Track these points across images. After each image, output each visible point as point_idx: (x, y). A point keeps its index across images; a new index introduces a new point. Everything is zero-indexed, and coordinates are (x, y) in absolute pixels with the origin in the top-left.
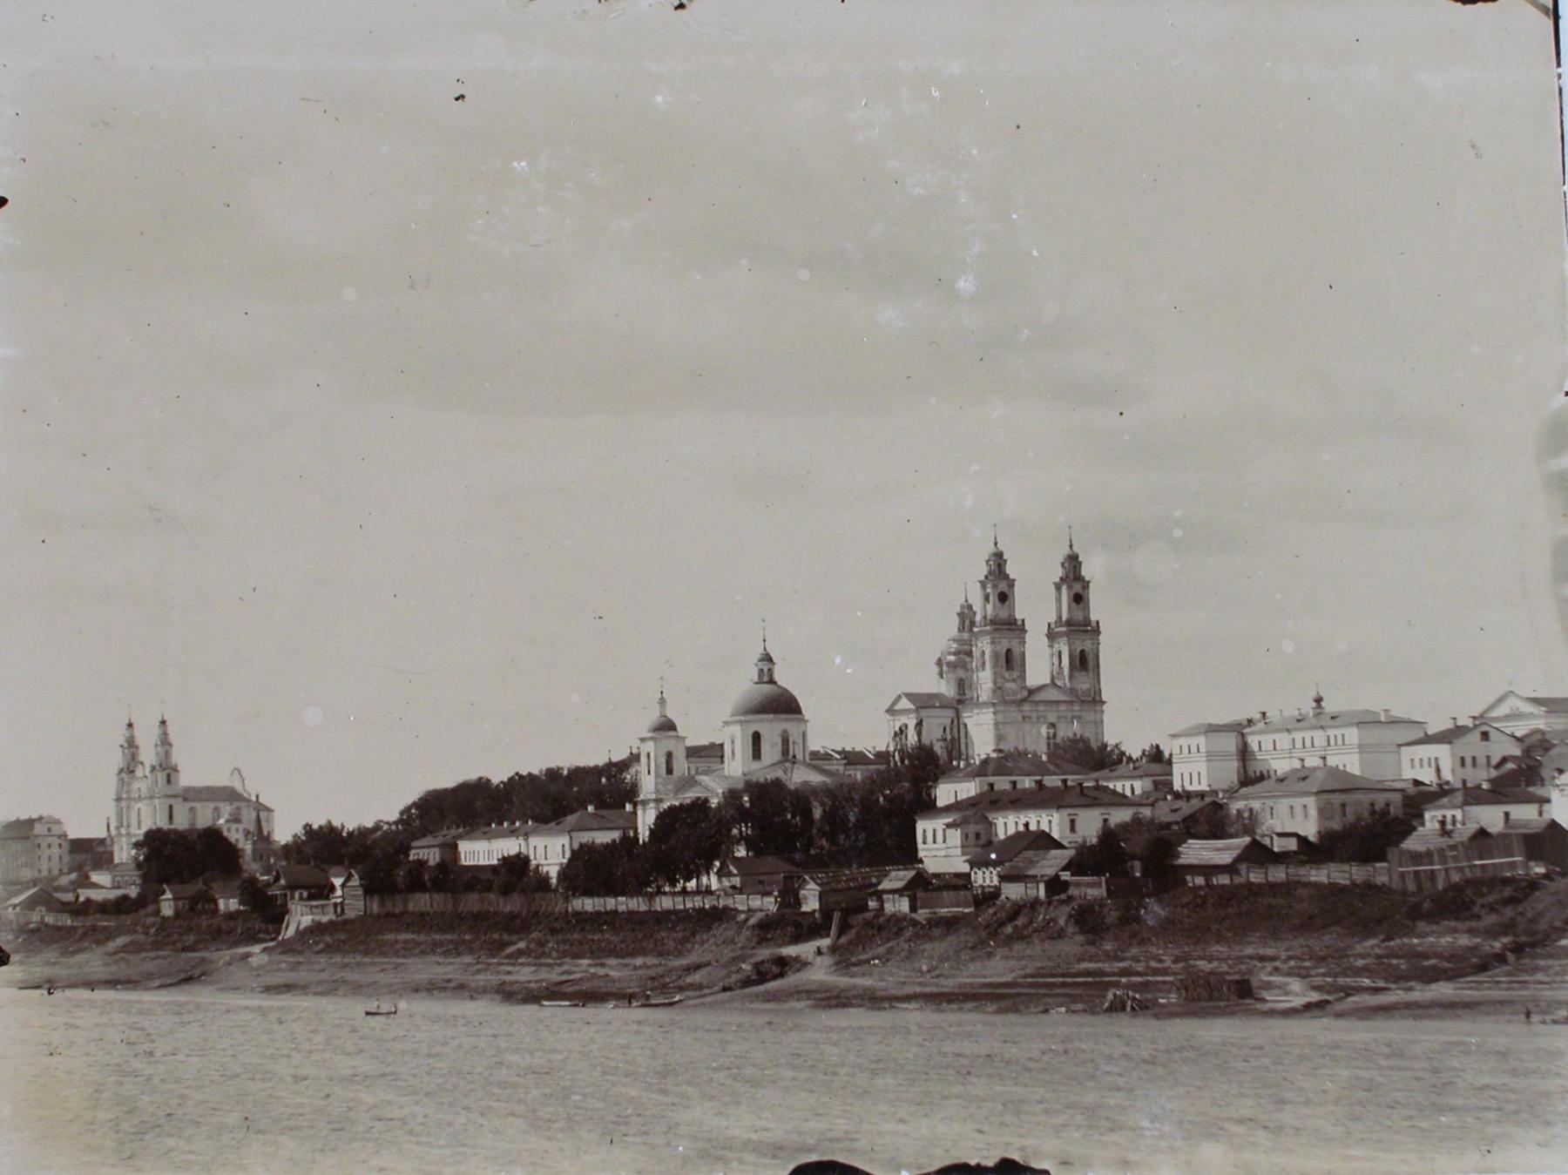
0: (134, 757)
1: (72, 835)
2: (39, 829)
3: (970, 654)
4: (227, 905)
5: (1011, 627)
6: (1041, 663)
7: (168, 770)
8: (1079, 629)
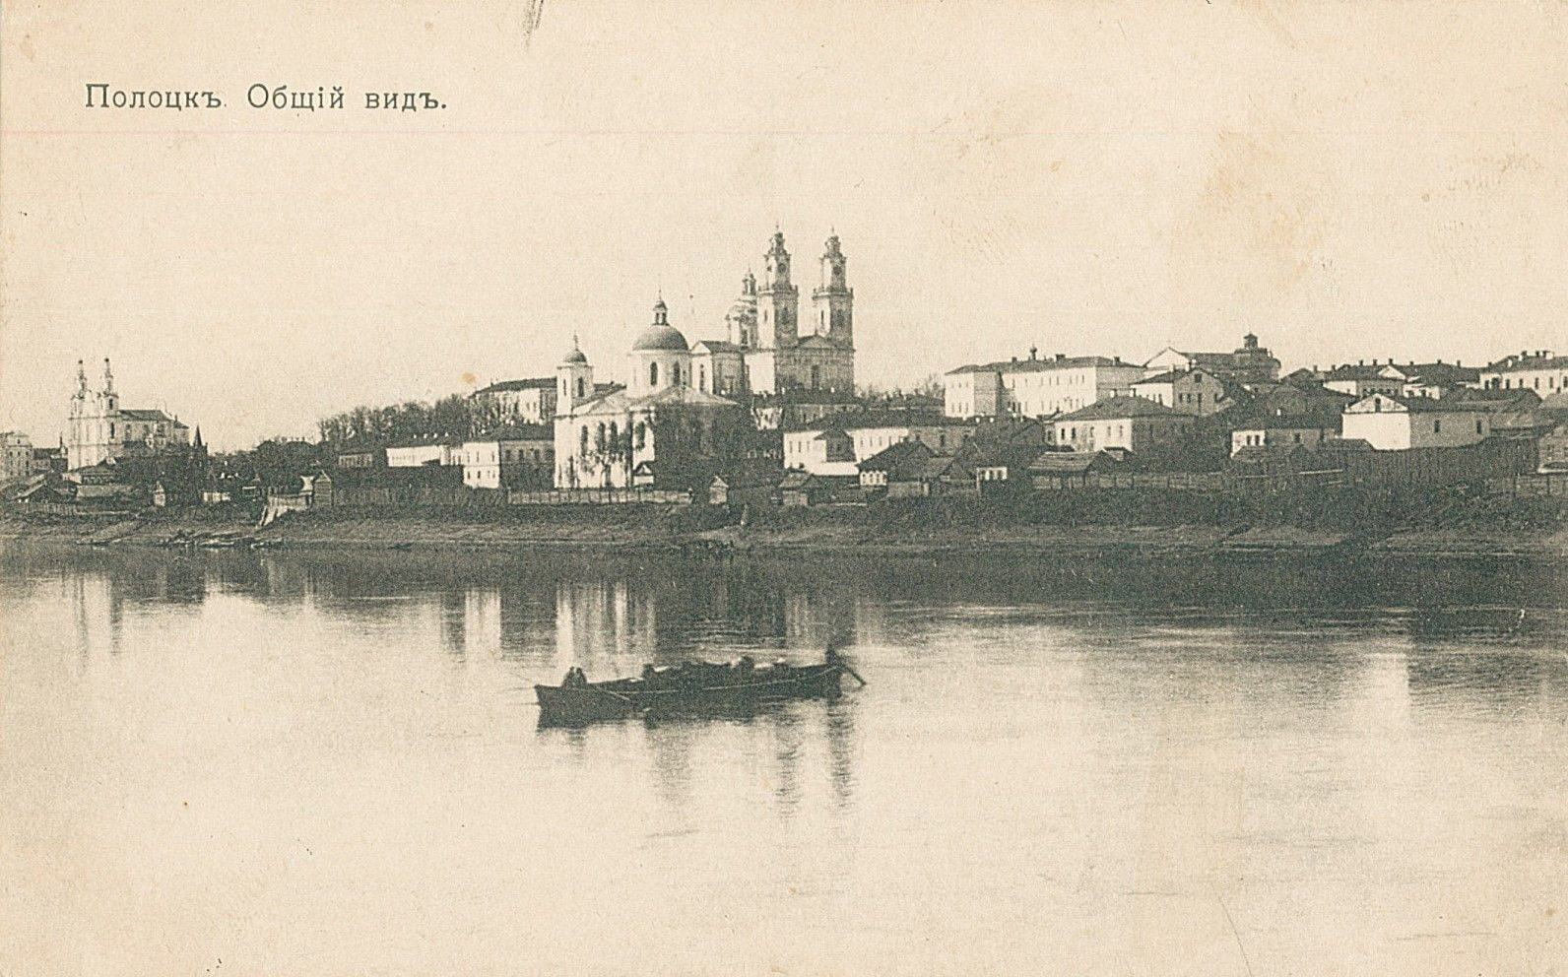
1: (35, 446)
3: (753, 311)
4: (210, 498)
5: (784, 291)
6: (812, 318)
7: (112, 399)
8: (839, 292)
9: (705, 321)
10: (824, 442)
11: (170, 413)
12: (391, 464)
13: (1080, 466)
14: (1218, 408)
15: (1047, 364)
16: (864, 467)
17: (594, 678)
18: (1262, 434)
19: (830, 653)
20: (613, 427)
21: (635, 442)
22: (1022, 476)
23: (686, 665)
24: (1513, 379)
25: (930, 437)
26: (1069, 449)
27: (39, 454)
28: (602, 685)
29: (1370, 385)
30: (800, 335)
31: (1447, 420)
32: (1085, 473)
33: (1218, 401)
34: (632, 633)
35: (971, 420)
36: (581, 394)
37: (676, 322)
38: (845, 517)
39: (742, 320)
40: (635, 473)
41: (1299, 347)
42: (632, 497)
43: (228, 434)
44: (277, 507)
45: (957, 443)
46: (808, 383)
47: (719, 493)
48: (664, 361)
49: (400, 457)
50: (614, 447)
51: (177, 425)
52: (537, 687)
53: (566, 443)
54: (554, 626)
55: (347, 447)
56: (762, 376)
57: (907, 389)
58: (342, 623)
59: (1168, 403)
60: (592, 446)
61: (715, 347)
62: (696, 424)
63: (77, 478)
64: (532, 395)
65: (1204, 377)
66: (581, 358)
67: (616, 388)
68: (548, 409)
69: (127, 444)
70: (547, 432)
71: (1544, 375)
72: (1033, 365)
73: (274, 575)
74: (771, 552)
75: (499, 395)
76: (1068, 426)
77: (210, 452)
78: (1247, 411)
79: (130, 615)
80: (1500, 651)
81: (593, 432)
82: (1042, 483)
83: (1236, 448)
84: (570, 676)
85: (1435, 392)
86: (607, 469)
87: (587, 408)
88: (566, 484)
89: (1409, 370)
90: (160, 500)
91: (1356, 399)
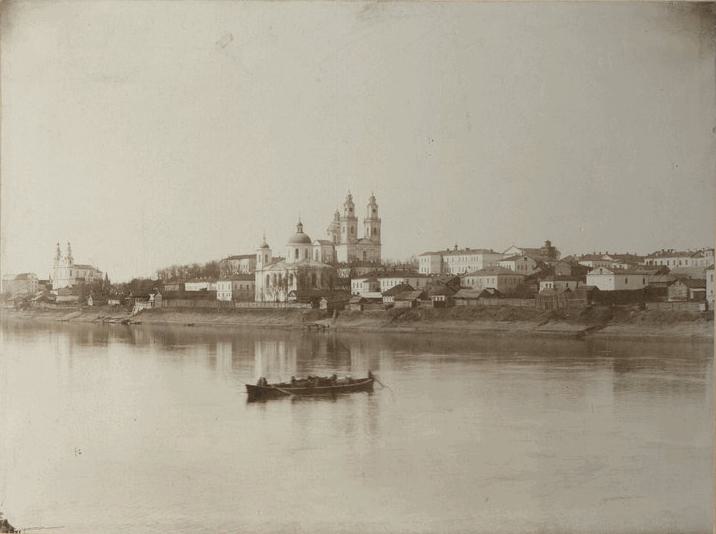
0: (59, 254)
2: (29, 276)
5: (352, 219)
6: (363, 232)
7: (70, 259)
9: (318, 232)
10: (367, 285)
11: (95, 266)
12: (187, 289)
13: (477, 295)
14: (534, 272)
15: (462, 252)
16: (386, 294)
17: (271, 382)
18: (552, 283)
19: (371, 376)
20: (280, 275)
21: (289, 283)
22: (451, 302)
23: (310, 378)
24: (658, 261)
25: (412, 282)
26: (470, 288)
27: (41, 282)
28: (276, 385)
29: (598, 263)
30: (359, 237)
31: (629, 277)
32: (477, 299)
33: (534, 269)
34: (286, 363)
35: (429, 276)
36: (266, 261)
37: (307, 231)
38: (377, 316)
39: (334, 231)
40: (289, 295)
41: (569, 248)
42: (288, 306)
43: (119, 276)
44: (139, 306)
45: (424, 285)
46: (361, 259)
47: (324, 305)
48: (302, 249)
49: (191, 287)
50: (280, 284)
51: (98, 272)
52: (248, 387)
53: (260, 281)
54: (254, 359)
55: (169, 282)
56: (342, 256)
57: (403, 261)
58: (168, 356)
59: (513, 269)
60: (271, 284)
61: (322, 243)
62: (314, 276)
63: (56, 293)
64: (245, 262)
65: (529, 259)
66: (267, 246)
67: (281, 259)
68: (253, 267)
69: (77, 279)
70: (252, 277)
71: (671, 260)
72: (456, 252)
73: (138, 335)
74: (345, 330)
75: (232, 261)
76: (471, 278)
77: (112, 283)
78: (547, 272)
79: (77, 349)
80: (653, 376)
81: (271, 277)
82: (459, 303)
83: (541, 289)
84: (260, 381)
85: (626, 266)
86: (277, 293)
87: (267, 268)
88: (260, 300)
89: (615, 257)
90: (90, 303)
91: (591, 269)
